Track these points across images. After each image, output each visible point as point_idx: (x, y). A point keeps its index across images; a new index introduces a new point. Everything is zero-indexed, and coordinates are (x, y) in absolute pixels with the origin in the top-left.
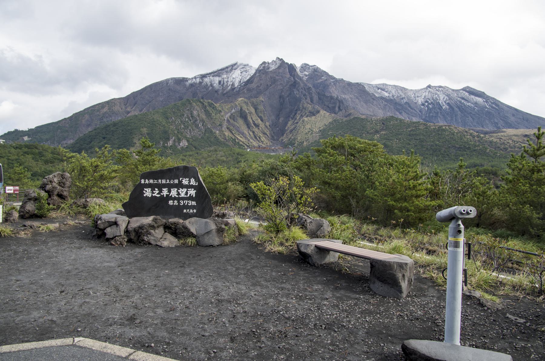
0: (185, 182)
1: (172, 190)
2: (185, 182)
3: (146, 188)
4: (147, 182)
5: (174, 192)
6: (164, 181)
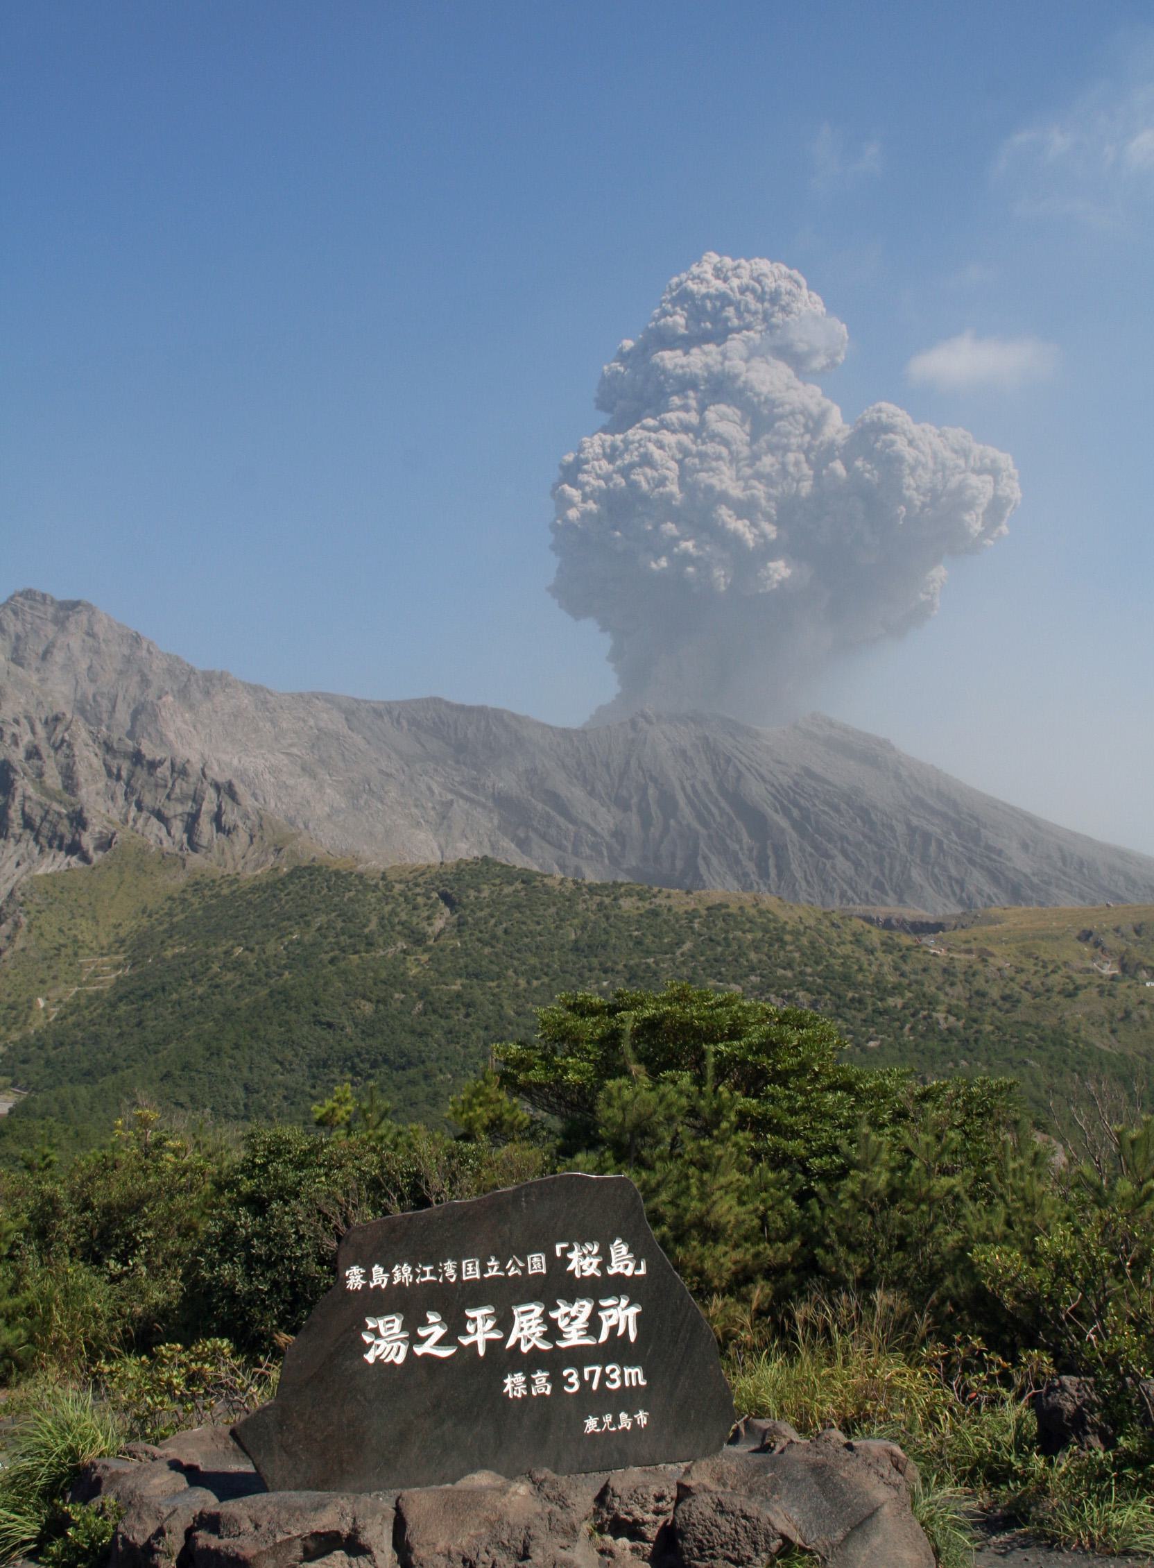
0: (583, 1262)
1: (517, 1311)
2: (583, 1262)
3: (377, 1314)
4: (379, 1277)
5: (527, 1327)
6: (471, 1271)
